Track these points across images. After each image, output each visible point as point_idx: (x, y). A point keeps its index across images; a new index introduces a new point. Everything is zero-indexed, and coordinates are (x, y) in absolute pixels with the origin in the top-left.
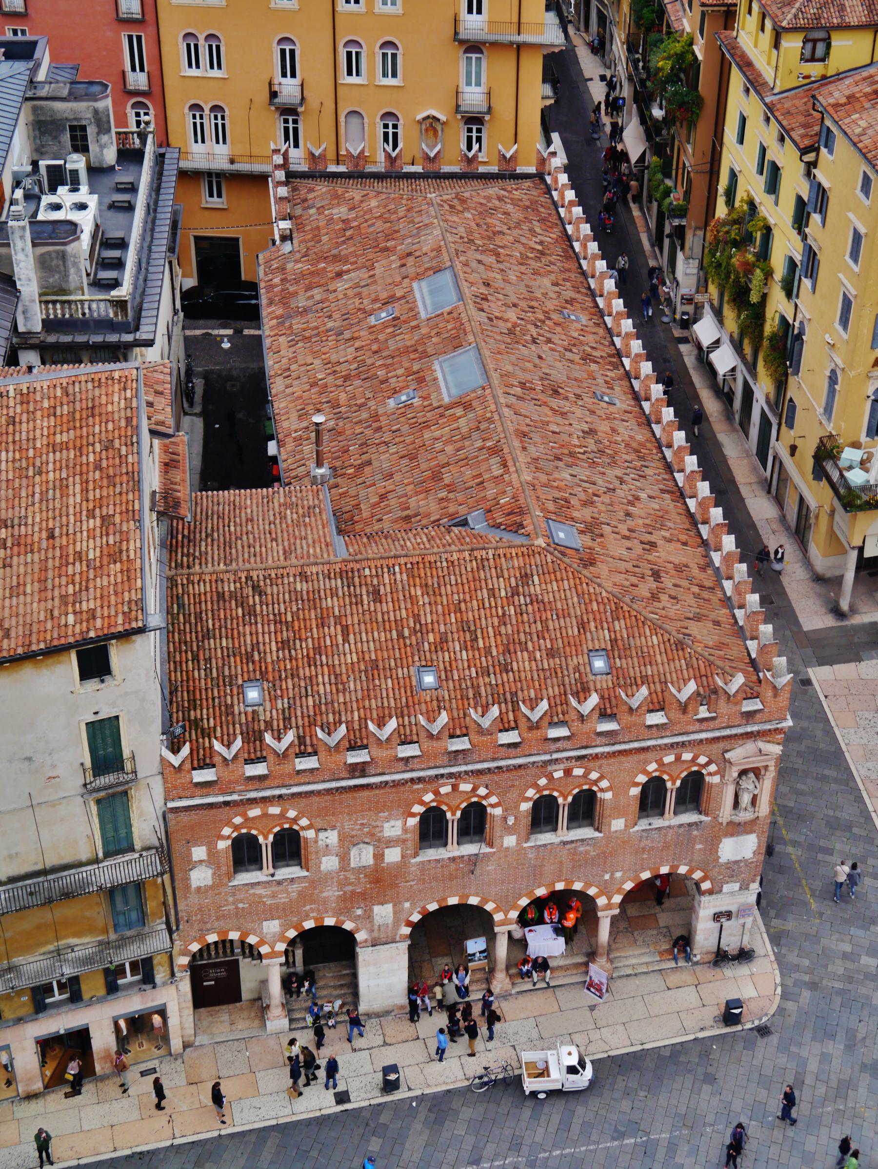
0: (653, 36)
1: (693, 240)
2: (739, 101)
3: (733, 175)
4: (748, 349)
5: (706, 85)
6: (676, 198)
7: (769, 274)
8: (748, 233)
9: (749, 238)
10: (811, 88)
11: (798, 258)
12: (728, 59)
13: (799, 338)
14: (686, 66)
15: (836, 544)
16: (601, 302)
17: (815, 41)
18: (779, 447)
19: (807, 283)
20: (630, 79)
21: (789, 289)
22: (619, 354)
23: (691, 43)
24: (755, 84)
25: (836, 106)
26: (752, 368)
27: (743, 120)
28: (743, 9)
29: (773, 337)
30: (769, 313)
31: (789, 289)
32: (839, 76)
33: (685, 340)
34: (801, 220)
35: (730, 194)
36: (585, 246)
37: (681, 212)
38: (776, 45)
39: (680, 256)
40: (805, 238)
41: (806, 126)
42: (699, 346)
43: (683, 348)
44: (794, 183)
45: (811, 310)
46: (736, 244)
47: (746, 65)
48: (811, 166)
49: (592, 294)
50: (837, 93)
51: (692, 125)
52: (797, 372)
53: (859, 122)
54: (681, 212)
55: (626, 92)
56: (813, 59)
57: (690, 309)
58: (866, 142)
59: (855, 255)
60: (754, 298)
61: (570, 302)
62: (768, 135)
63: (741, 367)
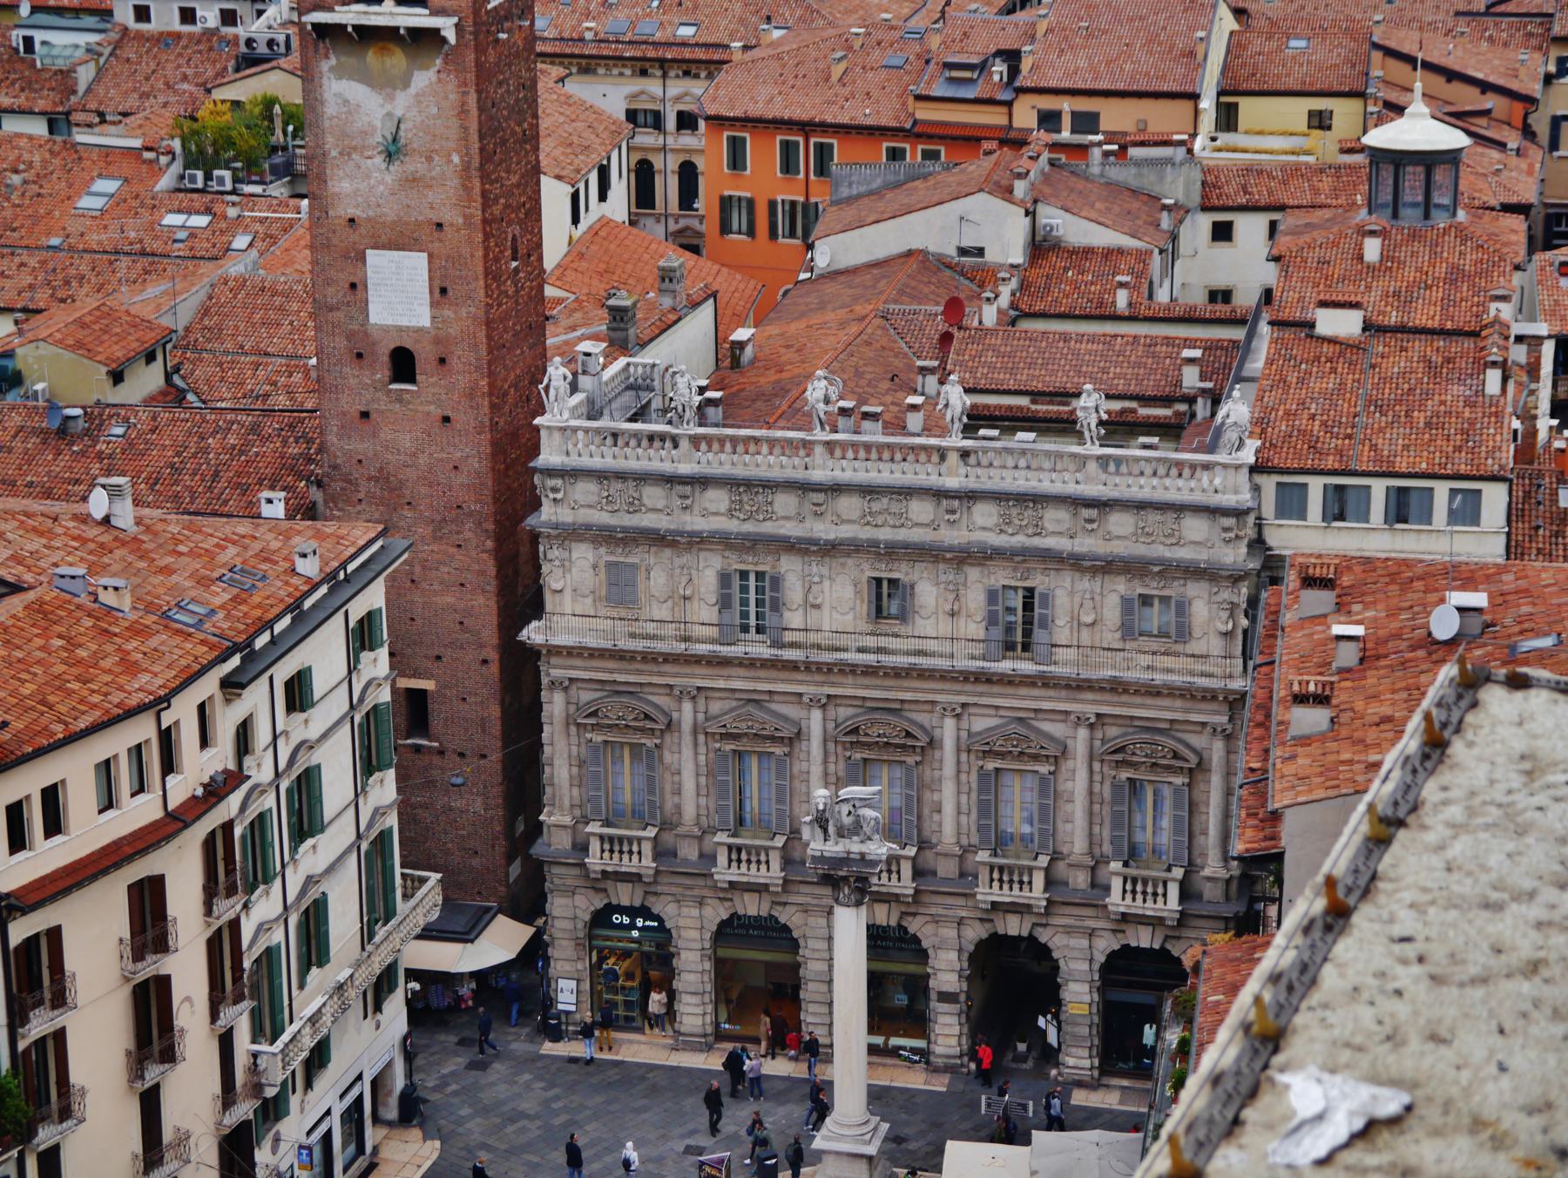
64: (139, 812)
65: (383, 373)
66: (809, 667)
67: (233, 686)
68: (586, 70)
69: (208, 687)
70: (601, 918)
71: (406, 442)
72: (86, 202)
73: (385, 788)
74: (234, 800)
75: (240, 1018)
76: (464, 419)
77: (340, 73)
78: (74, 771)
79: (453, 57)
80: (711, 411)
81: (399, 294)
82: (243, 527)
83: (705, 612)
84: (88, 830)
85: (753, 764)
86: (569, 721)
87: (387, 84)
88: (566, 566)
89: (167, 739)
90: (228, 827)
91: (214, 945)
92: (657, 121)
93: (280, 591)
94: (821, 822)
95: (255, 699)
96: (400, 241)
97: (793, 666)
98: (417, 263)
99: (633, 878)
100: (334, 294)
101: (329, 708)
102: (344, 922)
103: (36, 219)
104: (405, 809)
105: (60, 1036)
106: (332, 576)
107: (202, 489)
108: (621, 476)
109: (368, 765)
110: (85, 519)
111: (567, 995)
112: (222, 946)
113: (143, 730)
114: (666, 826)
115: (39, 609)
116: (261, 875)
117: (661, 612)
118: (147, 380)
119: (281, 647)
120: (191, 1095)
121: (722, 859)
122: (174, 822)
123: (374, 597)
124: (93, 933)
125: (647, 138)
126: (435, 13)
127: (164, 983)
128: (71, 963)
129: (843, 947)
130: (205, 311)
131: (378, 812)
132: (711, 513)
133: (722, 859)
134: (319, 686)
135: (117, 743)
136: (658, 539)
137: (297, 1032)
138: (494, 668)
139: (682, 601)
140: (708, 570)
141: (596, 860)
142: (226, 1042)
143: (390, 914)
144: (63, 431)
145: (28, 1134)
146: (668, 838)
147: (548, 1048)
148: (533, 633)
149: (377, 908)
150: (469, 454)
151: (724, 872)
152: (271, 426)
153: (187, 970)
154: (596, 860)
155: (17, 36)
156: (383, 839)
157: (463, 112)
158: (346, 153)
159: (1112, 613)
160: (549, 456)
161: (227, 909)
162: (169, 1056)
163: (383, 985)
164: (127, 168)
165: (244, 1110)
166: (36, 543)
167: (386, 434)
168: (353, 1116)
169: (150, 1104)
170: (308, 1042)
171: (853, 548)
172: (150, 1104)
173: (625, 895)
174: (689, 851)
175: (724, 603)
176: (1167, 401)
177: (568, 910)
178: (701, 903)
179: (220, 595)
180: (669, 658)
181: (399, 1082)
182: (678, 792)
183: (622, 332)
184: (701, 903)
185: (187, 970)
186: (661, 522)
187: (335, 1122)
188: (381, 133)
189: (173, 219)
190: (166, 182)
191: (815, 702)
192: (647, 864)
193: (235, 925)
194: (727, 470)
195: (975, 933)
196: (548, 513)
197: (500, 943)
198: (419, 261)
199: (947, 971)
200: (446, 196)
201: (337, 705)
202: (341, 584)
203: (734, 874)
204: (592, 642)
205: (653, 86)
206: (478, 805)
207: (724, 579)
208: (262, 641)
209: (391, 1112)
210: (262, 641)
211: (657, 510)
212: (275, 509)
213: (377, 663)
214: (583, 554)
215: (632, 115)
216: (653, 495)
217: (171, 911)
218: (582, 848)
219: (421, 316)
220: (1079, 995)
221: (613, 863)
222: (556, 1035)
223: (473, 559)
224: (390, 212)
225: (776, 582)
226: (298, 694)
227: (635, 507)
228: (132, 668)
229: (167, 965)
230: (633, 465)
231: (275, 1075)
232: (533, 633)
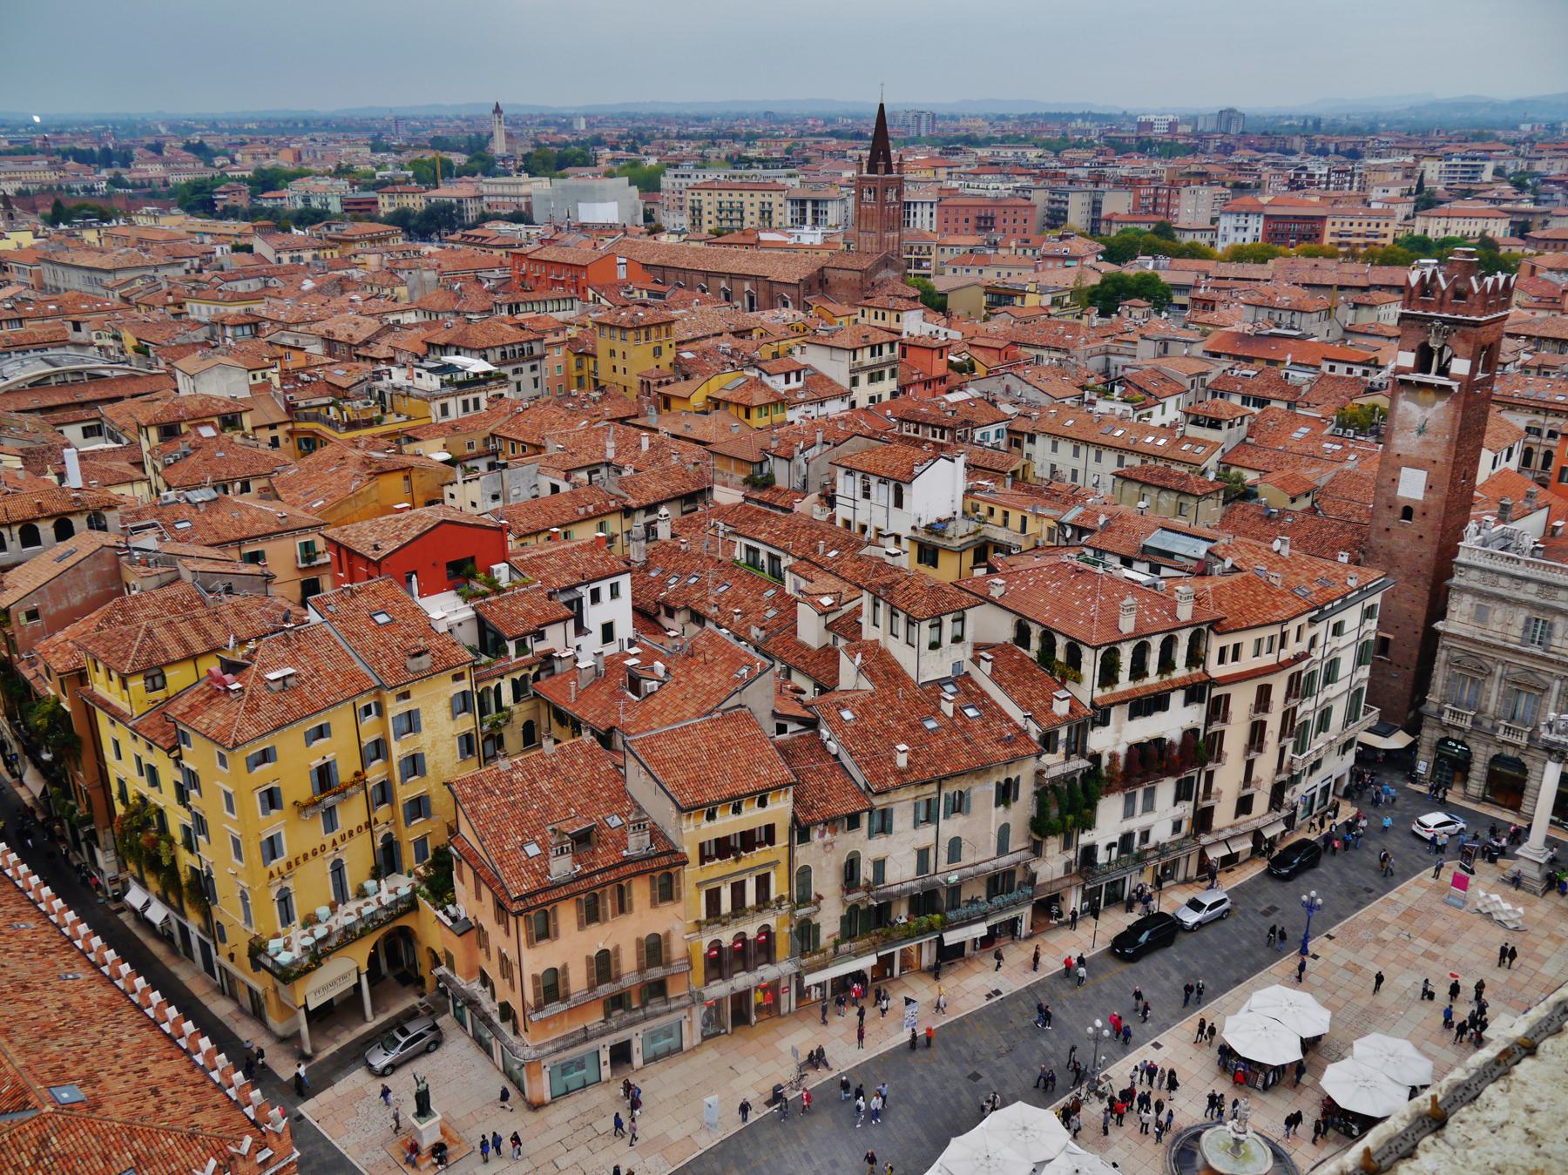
0: (26, 705)
1: (104, 837)
2: (108, 731)
3: (121, 783)
4: (173, 899)
5: (79, 726)
6: (81, 811)
7: (171, 841)
8: (146, 817)
9: (148, 822)
10: (161, 709)
11: (189, 824)
12: (90, 707)
13: (209, 877)
14: (59, 718)
15: (286, 1010)
16: (43, 907)
17: (153, 678)
18: (221, 959)
19: (202, 838)
20: (16, 739)
21: (190, 846)
22: (70, 940)
23: (58, 701)
24: (117, 716)
25: (183, 715)
26: (181, 911)
27: (116, 743)
28: (91, 669)
29: (189, 884)
30: (181, 868)
31: (190, 846)
32: (179, 695)
33: (122, 910)
34: (182, 795)
35: (123, 795)
36: (16, 871)
37: (89, 820)
38: (125, 687)
39: (98, 852)
40: (190, 808)
41: (164, 734)
42: (134, 910)
43: (122, 916)
44: (169, 775)
45: (212, 856)
46: (139, 829)
47: (106, 706)
48: (178, 760)
49: (34, 903)
50: (181, 706)
51: (77, 758)
52: (216, 902)
53: (203, 721)
54: (89, 820)
55: (16, 749)
56: (155, 689)
57: (118, 886)
58: (212, 732)
59: (230, 808)
60: (166, 862)
61: (17, 915)
62: (140, 747)
63: (172, 913)
64: (1268, 660)
65: (1398, 514)
66: (1558, 662)
67: (1313, 621)
68: (1511, 409)
69: (1304, 619)
70: (1443, 741)
71: (1402, 543)
72: (1296, 435)
73: (1365, 672)
74: (1305, 663)
75: (1289, 743)
76: (1428, 537)
77: (1406, 398)
78: (1247, 640)
79: (1455, 397)
80: (1537, 553)
81: (1412, 486)
82: (1330, 564)
83: (1516, 632)
84: (1248, 662)
85: (1524, 696)
86: (1447, 662)
87: (1424, 405)
88: (1459, 602)
89: (1284, 636)
90: (1300, 673)
91: (1285, 714)
92: (1539, 433)
93: (1340, 590)
94: (1550, 726)
95: (1321, 628)
96: (1417, 465)
97: (1552, 661)
100: (1385, 482)
101: (1349, 637)
102: (1337, 718)
103: (1275, 439)
104: (1371, 681)
105: (1222, 733)
106: (1360, 588)
107: (1318, 547)
108: (1491, 571)
109: (1360, 662)
110: (1270, 550)
111: (1422, 767)
112: (1288, 716)
113: (1275, 631)
114: (1480, 712)
115: (1247, 579)
116: (1308, 692)
117: (1498, 628)
118: (1305, 503)
119: (1334, 611)
120: (1266, 766)
121: (1501, 730)
122: (1280, 666)
123: (1376, 599)
124: (1242, 700)
125: (1533, 439)
126: (1452, 380)
127: (1264, 724)
128: (1231, 708)
130: (1332, 481)
131: (1360, 680)
132: (1529, 593)
133: (1501, 730)
134: (1346, 628)
135: (1265, 633)
136: (1502, 599)
137: (1310, 754)
138: (1420, 636)
139: (1506, 626)
140: (1521, 616)
141: (1446, 718)
142: (1282, 750)
143: (1356, 719)
144: (1269, 517)
145: (1204, 764)
146: (1479, 717)
147: (1410, 785)
148: (1439, 625)
149: (1352, 716)
150: (1428, 551)
151: (1501, 735)
152: (1349, 527)
153: (1273, 721)
154: (1446, 718)
155: (1283, 373)
156: (1360, 691)
157: (1454, 419)
158: (1402, 429)
160: (1462, 558)
161: (1293, 702)
162: (1260, 750)
163: (1347, 745)
164: (1314, 424)
165: (1284, 777)
166: (1250, 556)
167: (1395, 538)
168: (1325, 790)
169: (1250, 765)
170: (1314, 759)
172: (1250, 765)
173: (1455, 735)
174: (1487, 724)
175: (1526, 630)
177: (1430, 735)
178: (1488, 745)
179: (1316, 587)
180: (1496, 647)
181: (1346, 782)
182: (1488, 699)
183: (1504, 514)
184: (1488, 745)
185: (1273, 721)
186: (1505, 592)
187: (1318, 791)
188: (1418, 423)
190: (1327, 431)
191: (1558, 677)
192: (1468, 725)
193: (1295, 709)
194: (1539, 577)
196: (1456, 580)
197: (1398, 741)
198: (1424, 474)
200: (1439, 451)
201: (1353, 637)
202: (1364, 592)
203: (1505, 738)
204: (1464, 634)
205: (1540, 419)
206: (1401, 687)
207: (1528, 620)
208: (1328, 607)
209: (1341, 793)
210: (1328, 607)
211: (1504, 588)
212: (1344, 558)
213: (1372, 624)
214: (1468, 599)
215: (1528, 429)
216: (1503, 581)
217: (1272, 698)
218: (1441, 712)
221: (1453, 721)
222: (1414, 781)
223: (1421, 593)
224: (1415, 454)
225: (1551, 626)
226: (1338, 629)
227: (1495, 584)
228: (1276, 607)
229: (1266, 717)
230: (1498, 568)
231: (1298, 768)
232: (1439, 625)
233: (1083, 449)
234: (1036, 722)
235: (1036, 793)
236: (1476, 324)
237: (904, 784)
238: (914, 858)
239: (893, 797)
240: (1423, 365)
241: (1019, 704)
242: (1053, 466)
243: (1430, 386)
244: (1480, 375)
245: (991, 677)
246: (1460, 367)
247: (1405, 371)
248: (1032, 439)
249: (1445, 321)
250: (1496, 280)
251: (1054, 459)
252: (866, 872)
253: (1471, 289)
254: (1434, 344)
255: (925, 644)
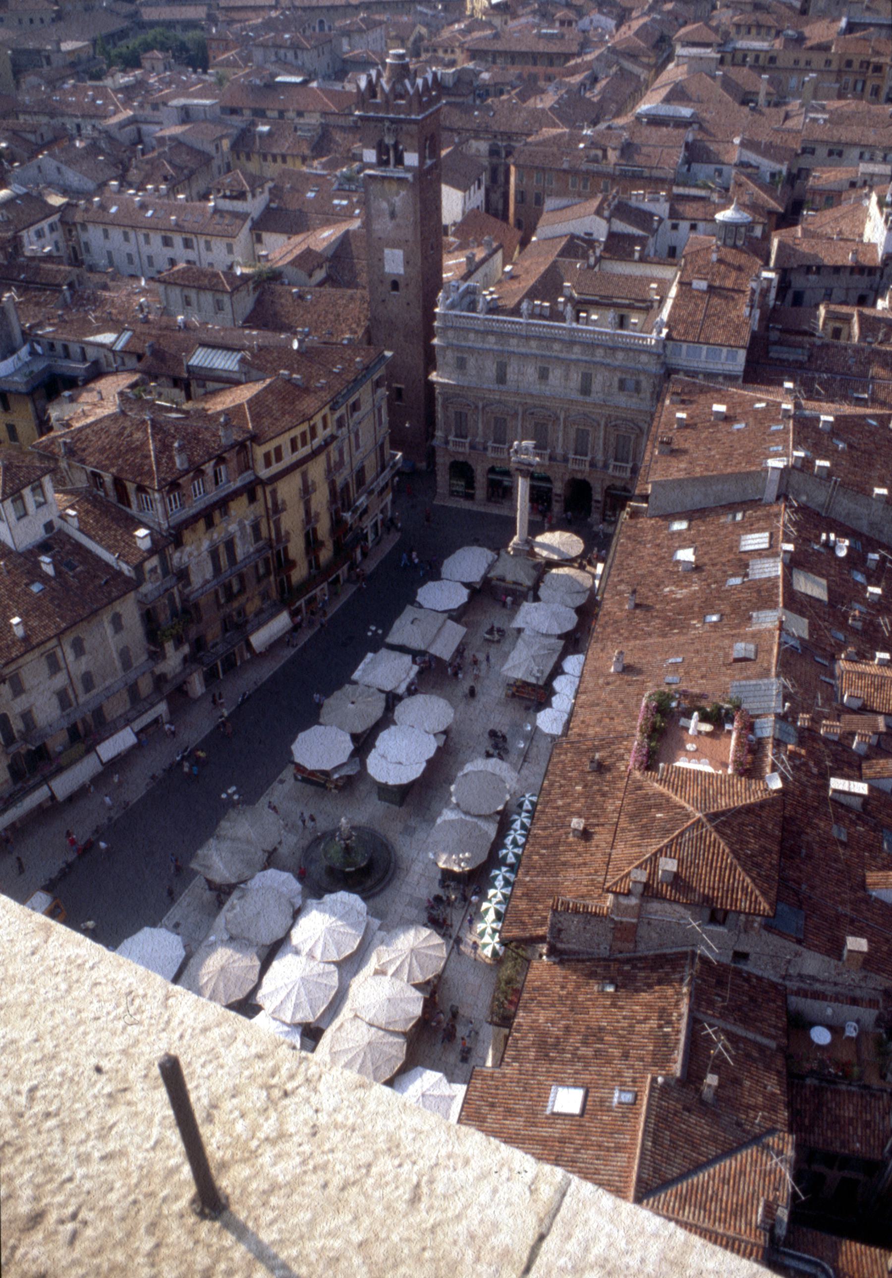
64: (303, 451)
67: (333, 409)
69: (326, 410)
81: (394, 262)
84: (289, 458)
96: (394, 245)
98: (399, 253)
99: (463, 453)
108: (463, 329)
113: (305, 427)
119: (350, 392)
129: (522, 487)
154: (451, 447)
159: (616, 384)
171: (535, 356)
176: (644, 301)
189: (336, 202)
195: (567, 477)
199: (558, 488)
219: (401, 271)
220: (598, 496)
233: (132, 235)
234: (127, 563)
235: (142, 616)
236: (415, 122)
237: (30, 649)
238: (55, 701)
239: (21, 661)
240: (382, 163)
241: (108, 548)
242: (109, 253)
243: (390, 179)
244: (429, 162)
245: (80, 530)
246: (411, 159)
247: (370, 166)
248: (84, 226)
249: (392, 121)
250: (425, 80)
251: (108, 245)
252: (17, 725)
253: (407, 91)
254: (389, 140)
255: (12, 518)
